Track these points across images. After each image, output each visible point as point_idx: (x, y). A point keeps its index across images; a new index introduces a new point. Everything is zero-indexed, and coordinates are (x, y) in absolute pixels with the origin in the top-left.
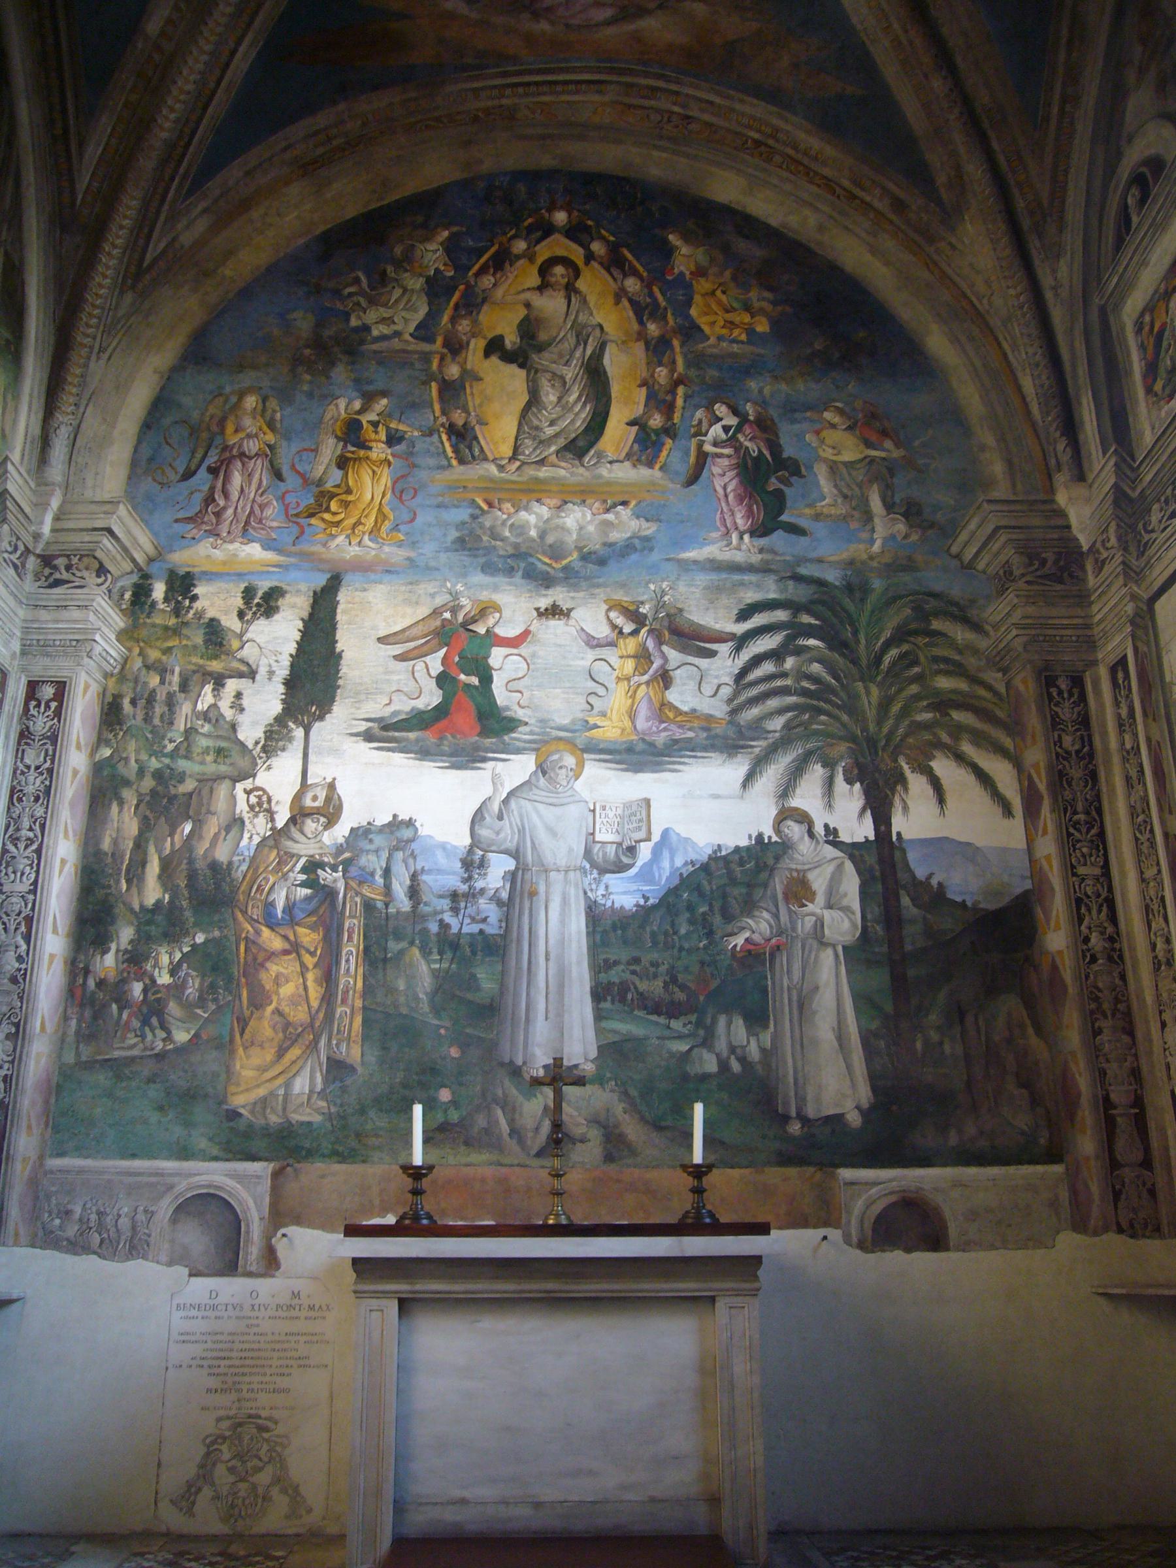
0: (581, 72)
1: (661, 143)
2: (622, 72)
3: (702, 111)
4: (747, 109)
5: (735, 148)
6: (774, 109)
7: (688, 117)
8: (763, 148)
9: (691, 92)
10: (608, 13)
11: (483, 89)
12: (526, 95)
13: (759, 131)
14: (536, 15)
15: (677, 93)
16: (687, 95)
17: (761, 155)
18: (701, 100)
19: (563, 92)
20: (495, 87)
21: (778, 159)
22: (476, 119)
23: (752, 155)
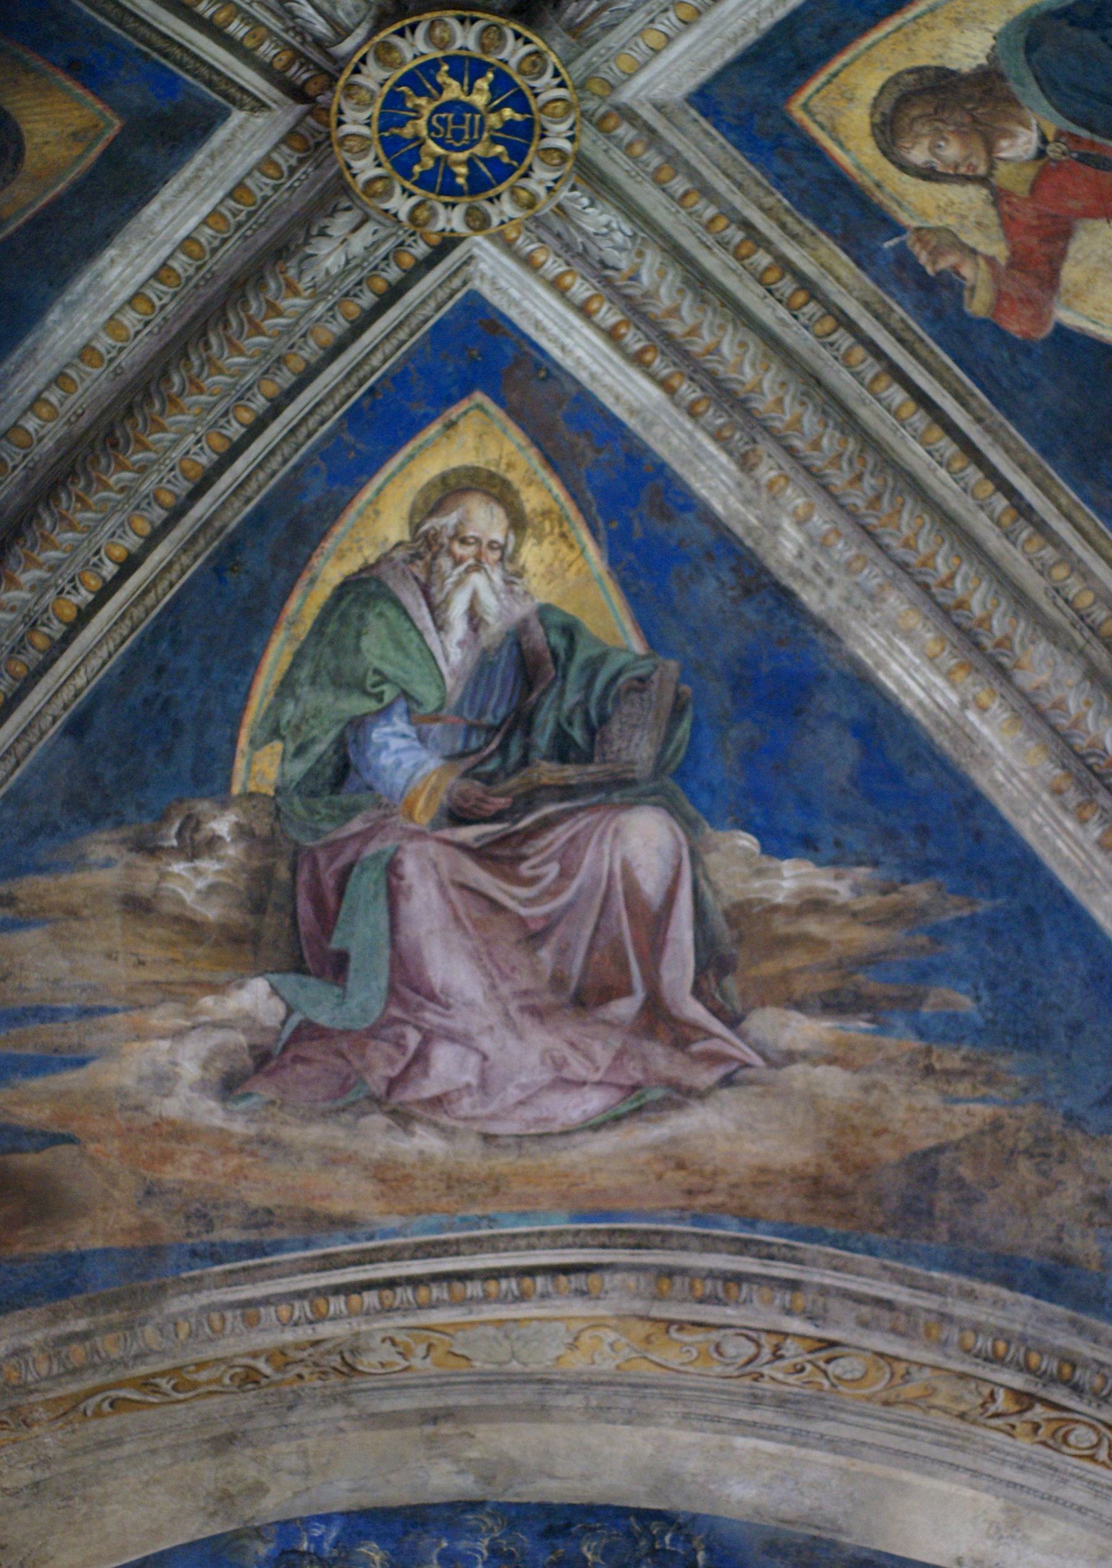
0: (531, 1247)
1: (755, 1415)
2: (641, 1241)
3: (864, 1324)
4: (981, 1313)
5: (962, 1416)
6: (1059, 1310)
7: (832, 1344)
8: (1039, 1412)
9: (829, 1279)
10: (594, 1101)
11: (267, 1301)
12: (387, 1310)
13: (1025, 1368)
14: (403, 1118)
15: (794, 1285)
16: (824, 1291)
17: (1036, 1427)
18: (860, 1299)
19: (486, 1298)
20: (301, 1295)
21: (1082, 1436)
22: (250, 1378)
23: (1010, 1431)
